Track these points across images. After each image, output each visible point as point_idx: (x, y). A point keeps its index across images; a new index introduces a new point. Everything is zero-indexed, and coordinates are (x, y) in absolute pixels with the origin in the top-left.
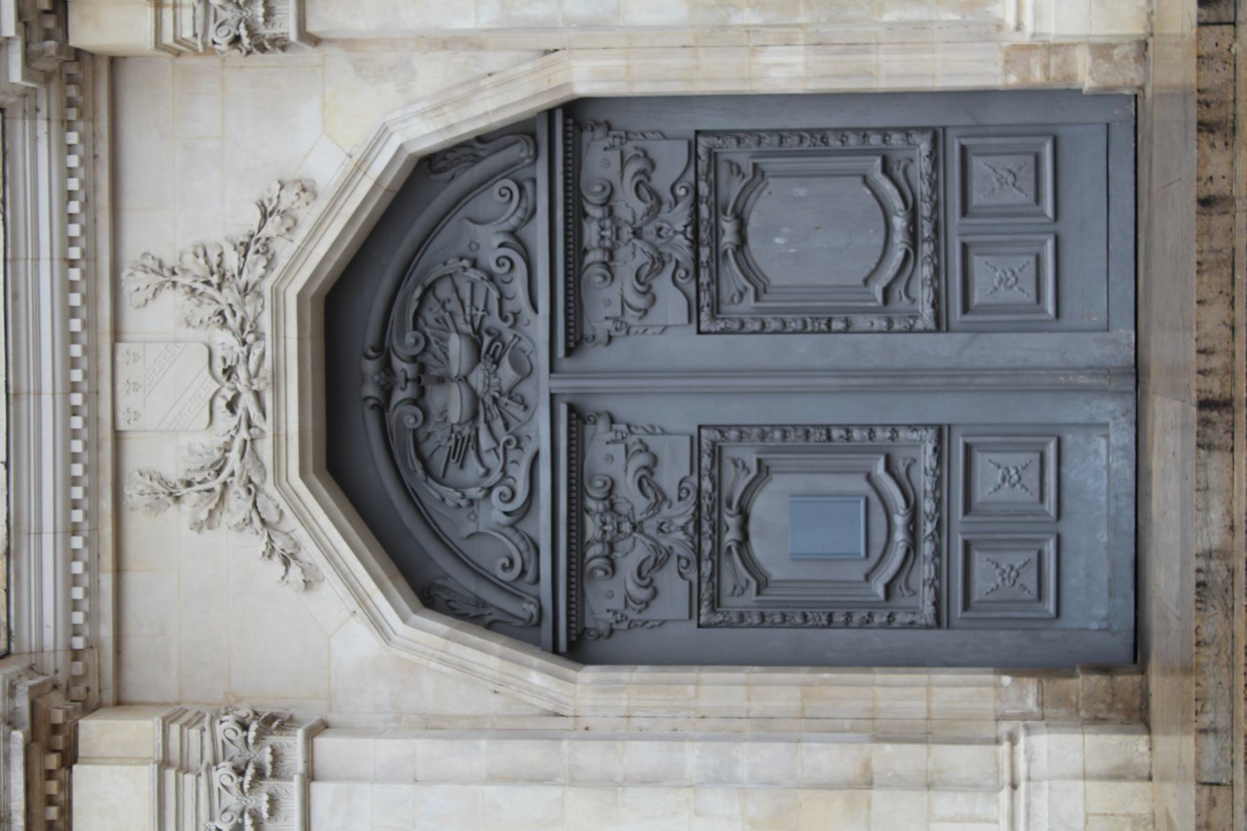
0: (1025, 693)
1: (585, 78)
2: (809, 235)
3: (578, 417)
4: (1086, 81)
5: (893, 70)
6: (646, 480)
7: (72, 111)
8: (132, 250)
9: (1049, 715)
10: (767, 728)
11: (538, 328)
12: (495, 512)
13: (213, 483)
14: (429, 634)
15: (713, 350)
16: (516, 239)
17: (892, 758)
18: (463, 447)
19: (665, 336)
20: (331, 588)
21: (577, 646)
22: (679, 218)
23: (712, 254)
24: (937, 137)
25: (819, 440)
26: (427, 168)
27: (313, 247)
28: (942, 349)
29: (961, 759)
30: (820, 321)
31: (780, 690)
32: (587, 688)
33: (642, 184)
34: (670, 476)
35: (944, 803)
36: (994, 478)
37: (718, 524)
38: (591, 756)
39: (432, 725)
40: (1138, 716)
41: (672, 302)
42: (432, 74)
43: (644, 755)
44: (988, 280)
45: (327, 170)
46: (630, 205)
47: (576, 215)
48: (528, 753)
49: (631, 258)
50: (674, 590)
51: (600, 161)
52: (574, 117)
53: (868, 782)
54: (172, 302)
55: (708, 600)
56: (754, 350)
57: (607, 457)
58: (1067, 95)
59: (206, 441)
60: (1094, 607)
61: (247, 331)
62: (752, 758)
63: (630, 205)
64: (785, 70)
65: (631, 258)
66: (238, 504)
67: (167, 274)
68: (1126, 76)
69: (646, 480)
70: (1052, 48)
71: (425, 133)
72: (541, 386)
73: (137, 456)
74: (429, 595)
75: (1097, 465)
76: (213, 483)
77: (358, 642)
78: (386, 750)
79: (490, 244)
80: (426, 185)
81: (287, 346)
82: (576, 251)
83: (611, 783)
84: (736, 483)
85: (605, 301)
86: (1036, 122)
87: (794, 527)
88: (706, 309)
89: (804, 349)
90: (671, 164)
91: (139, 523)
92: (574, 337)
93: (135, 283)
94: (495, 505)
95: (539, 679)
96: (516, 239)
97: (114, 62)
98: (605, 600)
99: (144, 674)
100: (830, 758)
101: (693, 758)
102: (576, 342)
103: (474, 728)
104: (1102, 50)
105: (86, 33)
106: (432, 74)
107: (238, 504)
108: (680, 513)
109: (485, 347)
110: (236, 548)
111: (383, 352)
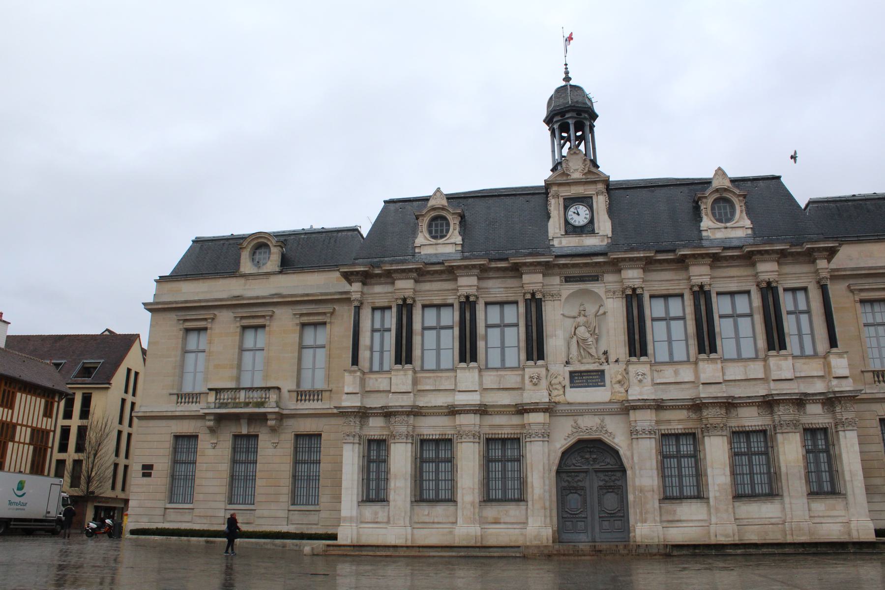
0: (555, 529)
1: (629, 472)
2: (611, 501)
3: (586, 472)
4: (632, 535)
5: (631, 511)
6: (579, 481)
7: (622, 409)
8: (606, 417)
9: (554, 532)
10: (550, 496)
11: (597, 467)
12: (574, 462)
13: (577, 427)
14: (559, 454)
15: (596, 489)
16: (608, 464)
17: (548, 511)
18: (582, 457)
19: (597, 483)
20: (565, 442)
21: (558, 472)
22: (612, 484)
23: (607, 488)
24: (623, 517)
25: (585, 502)
26: (617, 452)
27: (607, 439)
28: (597, 517)
29: (548, 520)
30: (600, 503)
31: (554, 498)
32: (554, 474)
33: (616, 480)
34: (580, 484)
35: (543, 518)
36: (581, 525)
37: (575, 490)
38: (547, 475)
39: (549, 455)
40: (553, 542)
41: (601, 483)
42: (628, 454)
43: (547, 482)
44: (606, 523)
45: (616, 441)
46: (613, 478)
47: (612, 471)
48: (547, 468)
49: (607, 478)
50: (565, 484)
51: (619, 474)
52: (624, 471)
53: (545, 509)
54: (599, 421)
55: (564, 488)
56: (596, 494)
57: (582, 475)
58: (629, 533)
59: (582, 426)
60: (566, 537)
61: (596, 431)
62: (547, 495)
63: (613, 478)
64: (631, 497)
65: (607, 478)
66: (575, 430)
67: (602, 421)
68: (631, 540)
69: (579, 481)
70: (635, 531)
71: (621, 452)
72: (591, 467)
73: (580, 418)
74: (564, 453)
75: (583, 537)
76: (577, 427)
77: (558, 445)
78: (546, 450)
79: (608, 460)
80: (615, 453)
81: (594, 436)
82: (607, 471)
83: (544, 477)
84: (579, 492)
85: (601, 475)
86: (626, 529)
87: (574, 500)
88: (601, 488)
89: (596, 500)
90: (619, 483)
91: (571, 418)
92: (596, 471)
93: (601, 417)
94: (576, 462)
95: (555, 468)
96: (608, 464)
97: (628, 414)
98: (564, 476)
99: (554, 418)
100: (547, 504)
101: (547, 488)
102: (596, 472)
103: (549, 460)
104: (635, 537)
105: (631, 412)
106: (628, 454)
107: (575, 430)
108: (575, 485)
109: (595, 460)
110: (569, 430)
111: (594, 447)
